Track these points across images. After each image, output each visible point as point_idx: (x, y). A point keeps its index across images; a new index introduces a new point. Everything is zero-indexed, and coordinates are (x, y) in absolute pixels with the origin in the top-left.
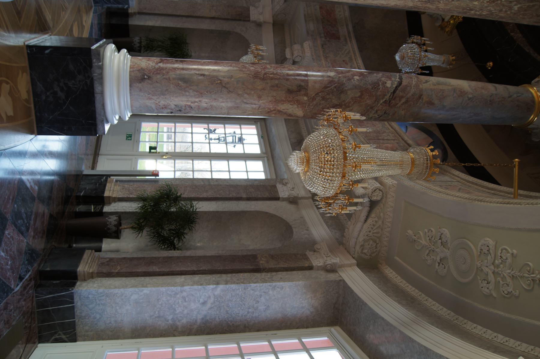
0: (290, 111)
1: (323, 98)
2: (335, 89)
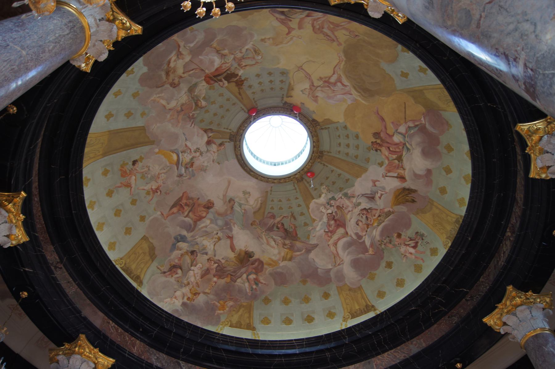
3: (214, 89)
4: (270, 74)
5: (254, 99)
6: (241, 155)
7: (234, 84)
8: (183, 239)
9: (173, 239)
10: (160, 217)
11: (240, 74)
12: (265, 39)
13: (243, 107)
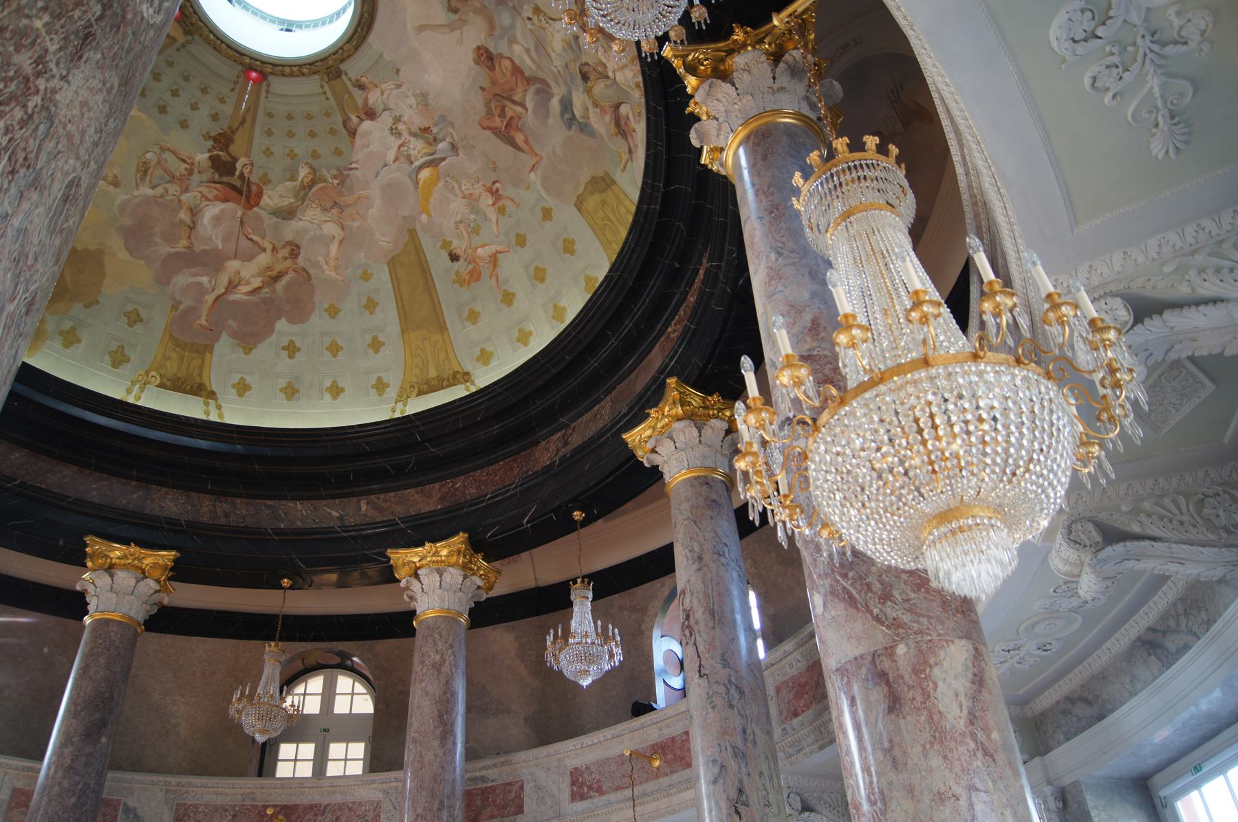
0: (962, 685)
1: (886, 597)
2: (851, 574)
3: (265, 175)
4: (163, 110)
5: (233, 90)
6: (349, 41)
7: (233, 149)
8: (566, 105)
9: (571, 132)
10: (539, 172)
11: (207, 155)
12: (110, 184)
13: (263, 91)
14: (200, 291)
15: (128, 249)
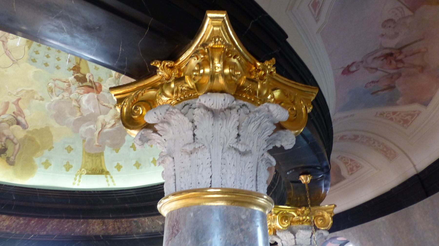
3: (99, 78)
4: (46, 65)
7: (82, 71)
11: (73, 77)
12: (40, 100)
14: (91, 132)
15: (59, 123)
